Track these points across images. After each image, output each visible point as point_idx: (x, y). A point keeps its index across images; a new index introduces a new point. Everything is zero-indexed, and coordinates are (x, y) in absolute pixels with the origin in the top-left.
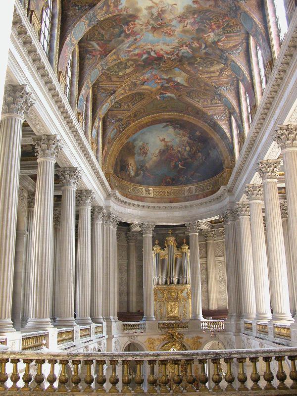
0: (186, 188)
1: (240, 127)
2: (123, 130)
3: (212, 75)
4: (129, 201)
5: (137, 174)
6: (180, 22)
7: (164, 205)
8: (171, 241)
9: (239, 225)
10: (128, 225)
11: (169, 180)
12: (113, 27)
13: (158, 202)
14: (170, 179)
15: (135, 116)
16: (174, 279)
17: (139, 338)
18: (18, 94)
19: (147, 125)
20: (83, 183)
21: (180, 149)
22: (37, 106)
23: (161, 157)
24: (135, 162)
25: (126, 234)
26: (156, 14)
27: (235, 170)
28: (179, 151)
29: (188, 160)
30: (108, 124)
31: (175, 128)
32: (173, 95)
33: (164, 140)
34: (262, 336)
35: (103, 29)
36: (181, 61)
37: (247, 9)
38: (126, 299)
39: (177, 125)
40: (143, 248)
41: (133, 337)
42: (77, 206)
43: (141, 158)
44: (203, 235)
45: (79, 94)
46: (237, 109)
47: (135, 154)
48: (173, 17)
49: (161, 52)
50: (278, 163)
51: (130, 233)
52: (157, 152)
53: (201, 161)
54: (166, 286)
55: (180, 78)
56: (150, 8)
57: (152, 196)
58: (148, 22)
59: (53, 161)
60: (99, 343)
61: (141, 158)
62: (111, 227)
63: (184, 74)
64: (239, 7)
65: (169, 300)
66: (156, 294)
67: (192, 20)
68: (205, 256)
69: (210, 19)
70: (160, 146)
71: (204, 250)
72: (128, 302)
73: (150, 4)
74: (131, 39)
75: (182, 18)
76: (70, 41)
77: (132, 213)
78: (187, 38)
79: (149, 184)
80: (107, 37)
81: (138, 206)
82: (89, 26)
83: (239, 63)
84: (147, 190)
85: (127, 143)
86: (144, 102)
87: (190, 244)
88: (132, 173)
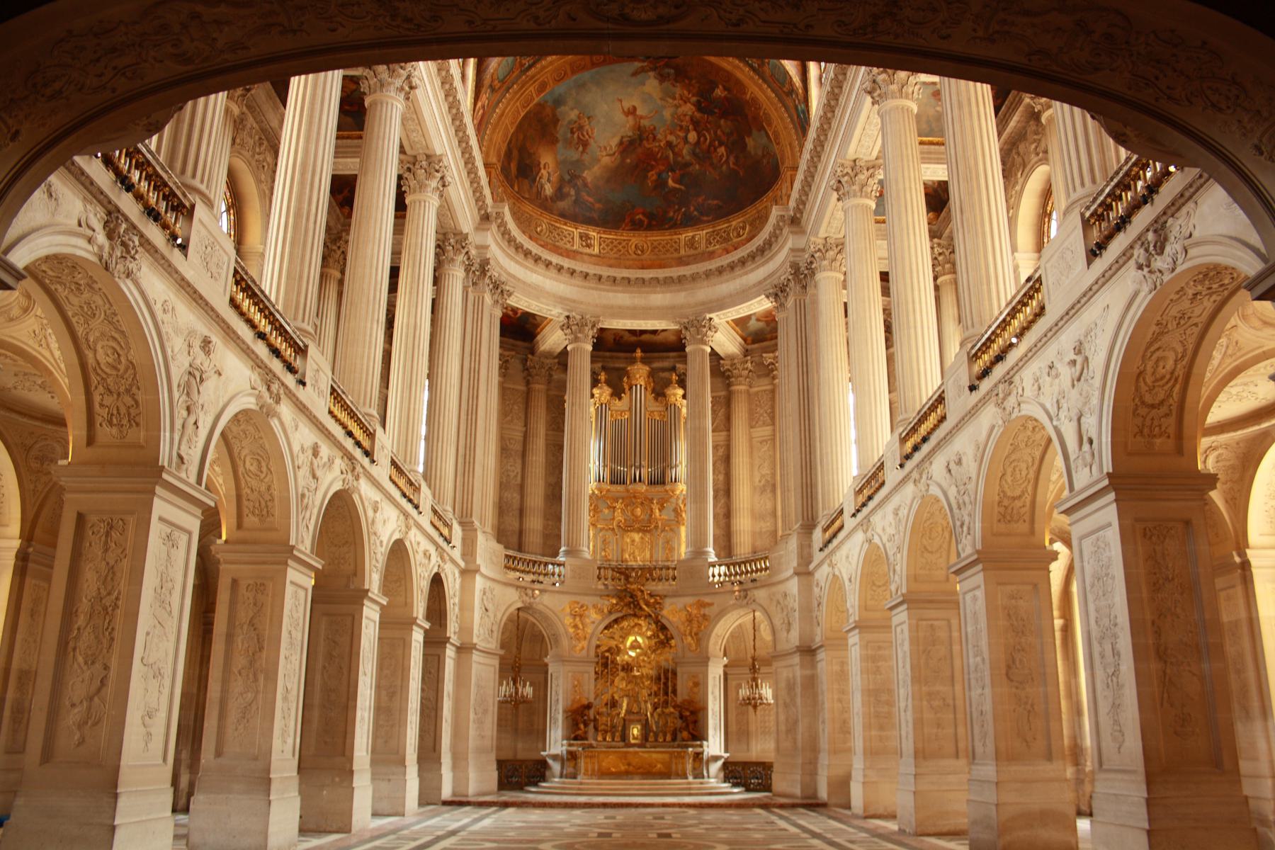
0: (685, 236)
2: (530, 67)
5: (559, 194)
9: (815, 302)
11: (640, 216)
13: (611, 266)
14: (644, 214)
21: (671, 138)
23: (623, 160)
24: (558, 163)
25: (525, 361)
27: (812, 134)
28: (669, 144)
29: (691, 168)
31: (662, 78)
33: (632, 112)
38: (516, 524)
39: (667, 70)
41: (530, 592)
43: (574, 155)
47: (557, 141)
51: (536, 359)
52: (614, 142)
53: (724, 167)
54: (620, 488)
57: (596, 251)
61: (574, 155)
65: (627, 528)
66: (595, 510)
68: (725, 423)
70: (625, 127)
71: (722, 412)
72: (521, 533)
77: (543, 290)
79: (589, 222)
81: (560, 269)
84: (585, 237)
85: (541, 106)
87: (689, 384)
88: (549, 190)
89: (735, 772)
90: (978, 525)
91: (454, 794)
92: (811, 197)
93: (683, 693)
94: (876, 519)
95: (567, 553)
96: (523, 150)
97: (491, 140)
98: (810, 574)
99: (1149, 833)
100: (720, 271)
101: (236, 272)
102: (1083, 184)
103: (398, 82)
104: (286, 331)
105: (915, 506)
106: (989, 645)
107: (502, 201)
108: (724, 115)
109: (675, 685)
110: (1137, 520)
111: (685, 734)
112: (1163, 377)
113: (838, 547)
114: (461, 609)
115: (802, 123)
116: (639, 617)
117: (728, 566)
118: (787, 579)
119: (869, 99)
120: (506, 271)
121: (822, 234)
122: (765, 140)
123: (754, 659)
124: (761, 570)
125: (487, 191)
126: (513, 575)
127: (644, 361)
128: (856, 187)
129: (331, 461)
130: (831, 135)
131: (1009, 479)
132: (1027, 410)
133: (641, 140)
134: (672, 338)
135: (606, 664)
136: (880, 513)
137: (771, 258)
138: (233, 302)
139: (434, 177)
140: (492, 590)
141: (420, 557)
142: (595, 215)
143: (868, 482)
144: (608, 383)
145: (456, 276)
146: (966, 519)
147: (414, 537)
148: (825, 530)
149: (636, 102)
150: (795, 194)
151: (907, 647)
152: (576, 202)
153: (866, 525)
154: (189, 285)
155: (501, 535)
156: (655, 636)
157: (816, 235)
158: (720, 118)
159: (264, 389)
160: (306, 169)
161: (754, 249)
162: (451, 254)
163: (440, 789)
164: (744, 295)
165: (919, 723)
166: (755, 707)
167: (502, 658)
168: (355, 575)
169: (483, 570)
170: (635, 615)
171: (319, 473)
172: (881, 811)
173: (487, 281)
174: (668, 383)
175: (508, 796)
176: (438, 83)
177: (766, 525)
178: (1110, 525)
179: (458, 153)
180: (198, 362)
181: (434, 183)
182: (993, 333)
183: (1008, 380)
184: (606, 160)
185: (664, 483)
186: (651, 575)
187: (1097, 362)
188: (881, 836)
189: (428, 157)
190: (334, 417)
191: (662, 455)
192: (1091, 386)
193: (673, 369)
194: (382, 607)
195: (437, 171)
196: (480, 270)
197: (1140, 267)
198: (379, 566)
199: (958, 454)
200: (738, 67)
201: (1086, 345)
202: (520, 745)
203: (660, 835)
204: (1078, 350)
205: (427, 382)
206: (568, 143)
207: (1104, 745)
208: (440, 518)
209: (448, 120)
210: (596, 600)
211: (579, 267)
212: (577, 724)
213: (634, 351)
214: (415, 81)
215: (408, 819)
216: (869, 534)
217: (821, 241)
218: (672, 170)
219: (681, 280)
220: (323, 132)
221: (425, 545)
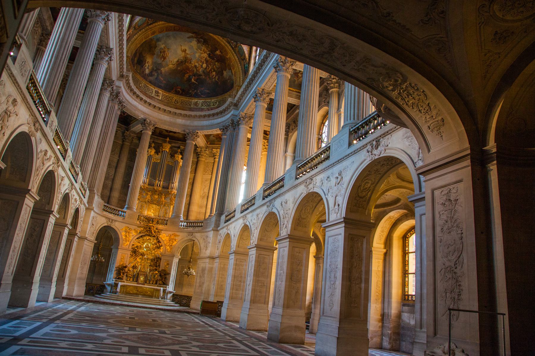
0: (194, 100)
2: (151, 24)
4: (138, 92)
5: (151, 74)
7: (170, 109)
9: (237, 135)
16: (162, 183)
17: (117, 223)
21: (197, 64)
23: (177, 67)
25: (123, 133)
27: (250, 77)
28: (195, 66)
31: (199, 42)
33: (185, 51)
38: (108, 194)
51: (128, 133)
52: (176, 60)
54: (151, 187)
61: (159, 61)
66: (140, 193)
68: (195, 171)
70: (180, 55)
72: (109, 197)
79: (160, 87)
81: (145, 102)
84: (157, 92)
85: (151, 39)
88: (147, 71)
89: (176, 298)
90: (290, 226)
91: (67, 295)
92: (244, 98)
93: (163, 265)
94: (249, 216)
95: (128, 208)
96: (141, 54)
97: (130, 47)
98: (218, 231)
99: (338, 338)
100: (205, 116)
101: (31, 75)
102: (350, 119)
103: (103, 16)
104: (44, 103)
105: (266, 215)
106: (287, 267)
107: (129, 71)
108: (218, 61)
109: (160, 263)
110: (350, 234)
111: (161, 282)
112: (366, 188)
113: (231, 223)
114: (83, 223)
115: (246, 71)
116: (150, 236)
117: (187, 223)
118: (209, 231)
119: (274, 70)
120: (125, 98)
121: (245, 112)
122: (230, 74)
123: (191, 258)
124: (199, 226)
125: (125, 67)
126: (105, 213)
127: (169, 142)
128: (262, 99)
129: (49, 159)
130: (256, 79)
131: (303, 212)
132: (316, 190)
133: (185, 62)
134: (181, 136)
135: (135, 252)
136: (251, 214)
137: (224, 116)
138: (28, 88)
139: (107, 56)
140: (96, 217)
141: (73, 201)
142: (162, 85)
143: (248, 202)
144: (154, 147)
145: (107, 95)
146: (286, 222)
147: (74, 192)
148: (226, 216)
149: (187, 48)
150: (238, 96)
151: (253, 263)
152: (156, 78)
153: (244, 217)
154: (13, 76)
155: (102, 197)
156: (155, 244)
157: (243, 112)
158: (216, 61)
159: (33, 124)
160: (63, 41)
161: (219, 111)
162: (106, 87)
163: (62, 292)
164: (211, 127)
165: (254, 290)
166: (188, 276)
167: (95, 244)
168: (49, 204)
169: (95, 209)
170: (149, 235)
171: (45, 162)
172: (232, 319)
173: (117, 100)
174: (176, 152)
175: (88, 298)
176: (117, 21)
178: (341, 234)
179: (118, 50)
180: (10, 108)
181: (107, 59)
182: (308, 161)
183: (311, 179)
184: (171, 66)
185: (168, 188)
186: (158, 221)
187: (346, 179)
188: (233, 329)
189: (107, 48)
190: (54, 141)
191: (169, 178)
192: (342, 187)
193: (179, 148)
194: (57, 219)
195: (109, 54)
196: (116, 96)
197: (368, 152)
198: (59, 202)
199: (286, 200)
200: (227, 46)
201: (343, 173)
202: (94, 278)
203: (154, 320)
204: (340, 174)
207: (325, 307)
208: (83, 187)
209: (117, 36)
211: (153, 103)
212: (120, 273)
213: (166, 138)
214: (110, 18)
215: (50, 304)
216: (245, 221)
217: (244, 114)
218: (195, 76)
220: (73, 28)
221: (76, 196)
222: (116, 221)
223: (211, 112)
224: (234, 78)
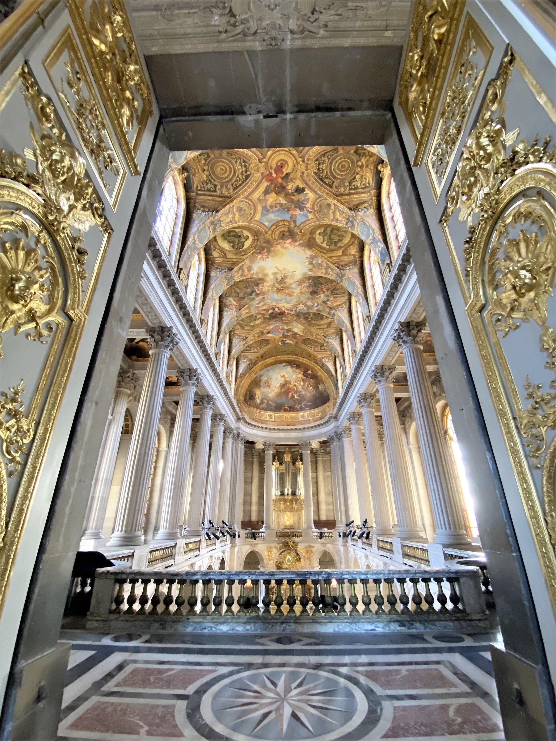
0: (301, 414)
1: (343, 367)
3: (322, 327)
5: (262, 402)
6: (299, 285)
8: (287, 458)
10: (253, 443)
12: (247, 288)
15: (262, 357)
18: (165, 333)
19: (271, 364)
20: (217, 408)
22: (181, 345)
26: (280, 278)
30: (240, 362)
31: (292, 367)
32: (291, 342)
33: (284, 376)
34: (367, 547)
35: (238, 288)
36: (298, 315)
37: (350, 276)
40: (264, 462)
42: (212, 427)
44: (314, 453)
45: (218, 338)
46: (341, 353)
48: (292, 281)
49: (283, 309)
50: (375, 395)
52: (278, 385)
54: (282, 497)
55: (298, 328)
56: (275, 274)
58: (274, 285)
59: (194, 389)
60: (224, 552)
62: (240, 445)
63: (300, 326)
64: (344, 275)
65: (285, 510)
67: (308, 284)
69: (321, 284)
70: (281, 381)
71: (314, 466)
73: (276, 271)
74: (260, 297)
75: (300, 282)
76: (212, 296)
78: (303, 298)
79: (271, 410)
80: (241, 295)
81: (262, 428)
82: (227, 285)
83: (343, 318)
84: (270, 415)
85: (256, 378)
86: (269, 346)
88: (258, 401)
100: (312, 427)
103: (210, 406)
108: (311, 378)
114: (230, 561)
133: (286, 384)
144: (278, 460)
177: (331, 507)
184: (276, 391)
205: (222, 461)
206: (264, 387)
210: (275, 544)
211: (268, 427)
219: (300, 429)
222: (257, 544)
223: (317, 423)
224: (328, 390)
